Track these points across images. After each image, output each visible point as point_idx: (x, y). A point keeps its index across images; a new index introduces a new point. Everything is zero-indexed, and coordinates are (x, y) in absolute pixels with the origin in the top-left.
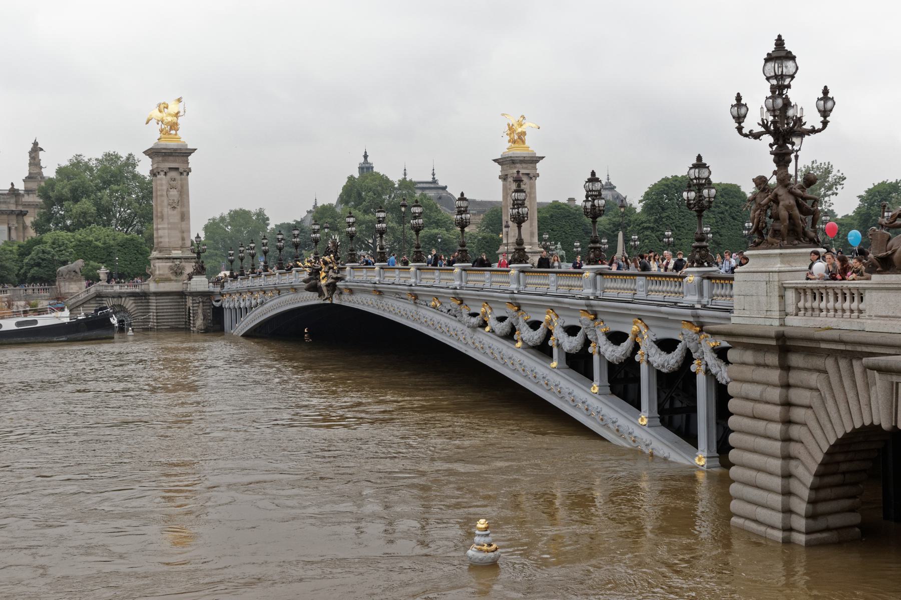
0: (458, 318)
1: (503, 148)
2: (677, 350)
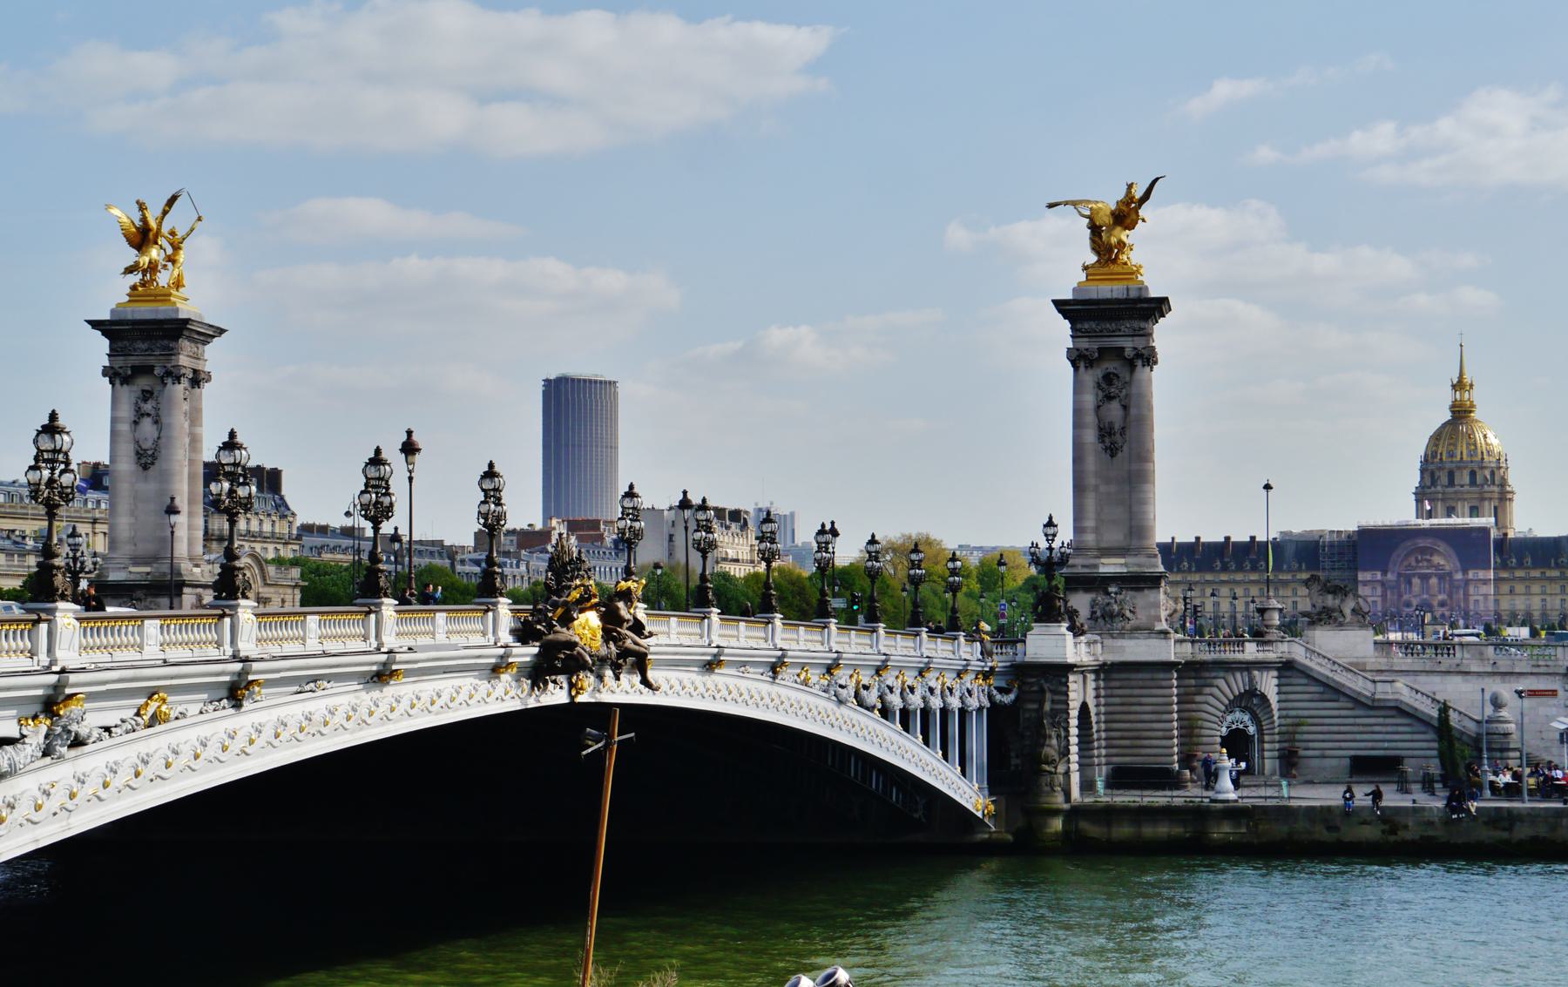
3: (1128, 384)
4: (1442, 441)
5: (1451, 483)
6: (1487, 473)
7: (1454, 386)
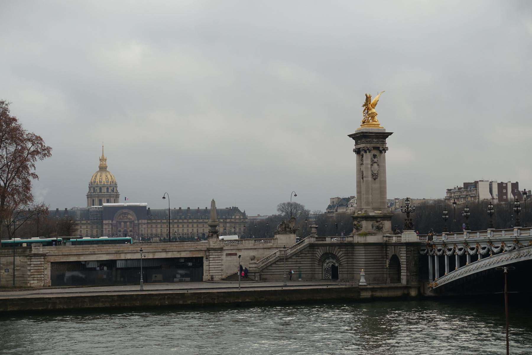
4: (97, 178)
5: (101, 191)
6: (112, 188)
7: (100, 160)
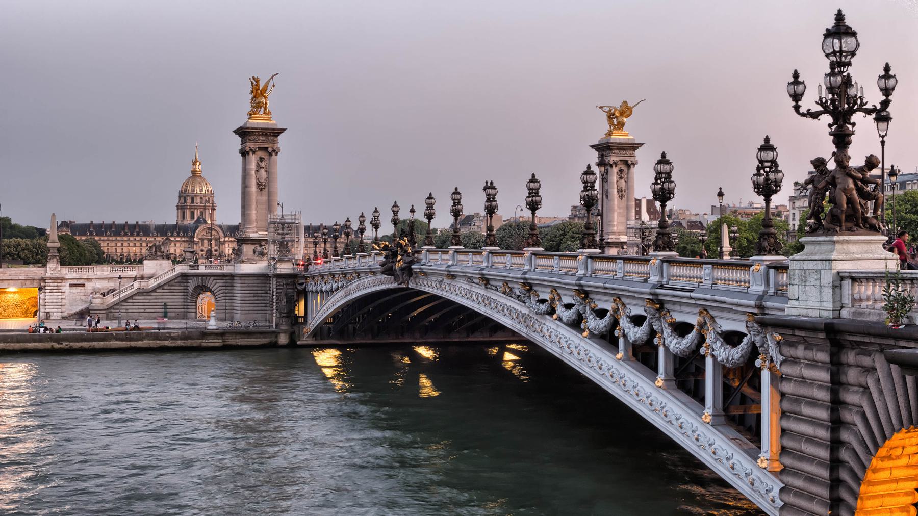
0: (527, 304)
1: (599, 130)
2: (742, 344)
3: (628, 173)
5: (193, 202)
6: (207, 198)
